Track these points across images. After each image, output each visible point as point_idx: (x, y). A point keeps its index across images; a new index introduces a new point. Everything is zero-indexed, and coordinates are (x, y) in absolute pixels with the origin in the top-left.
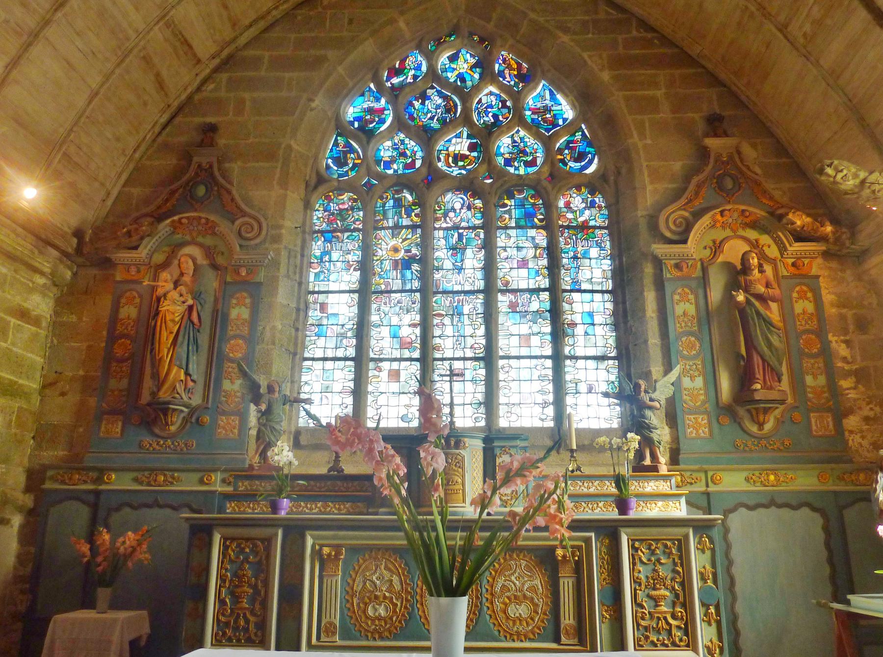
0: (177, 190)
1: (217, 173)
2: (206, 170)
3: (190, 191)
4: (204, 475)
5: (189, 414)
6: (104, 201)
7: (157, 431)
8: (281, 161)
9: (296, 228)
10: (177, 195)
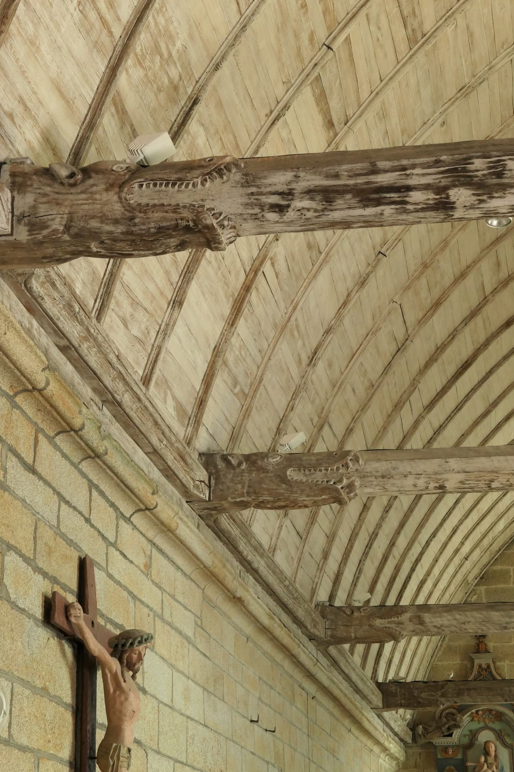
1: (494, 673)
2: (486, 670)
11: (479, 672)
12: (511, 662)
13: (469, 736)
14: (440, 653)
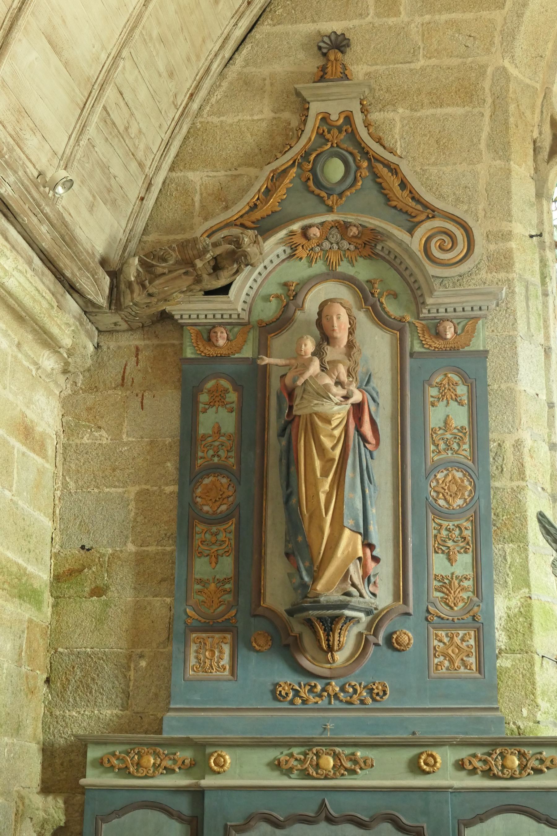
0: (285, 172)
1: (363, 133)
3: (313, 170)
4: (419, 756)
5: (369, 627)
6: (142, 199)
7: (306, 663)
8: (489, 100)
9: (531, 236)
10: (287, 181)
11: (321, 135)
12: (412, 110)
13: (277, 297)
14: (218, 95)
